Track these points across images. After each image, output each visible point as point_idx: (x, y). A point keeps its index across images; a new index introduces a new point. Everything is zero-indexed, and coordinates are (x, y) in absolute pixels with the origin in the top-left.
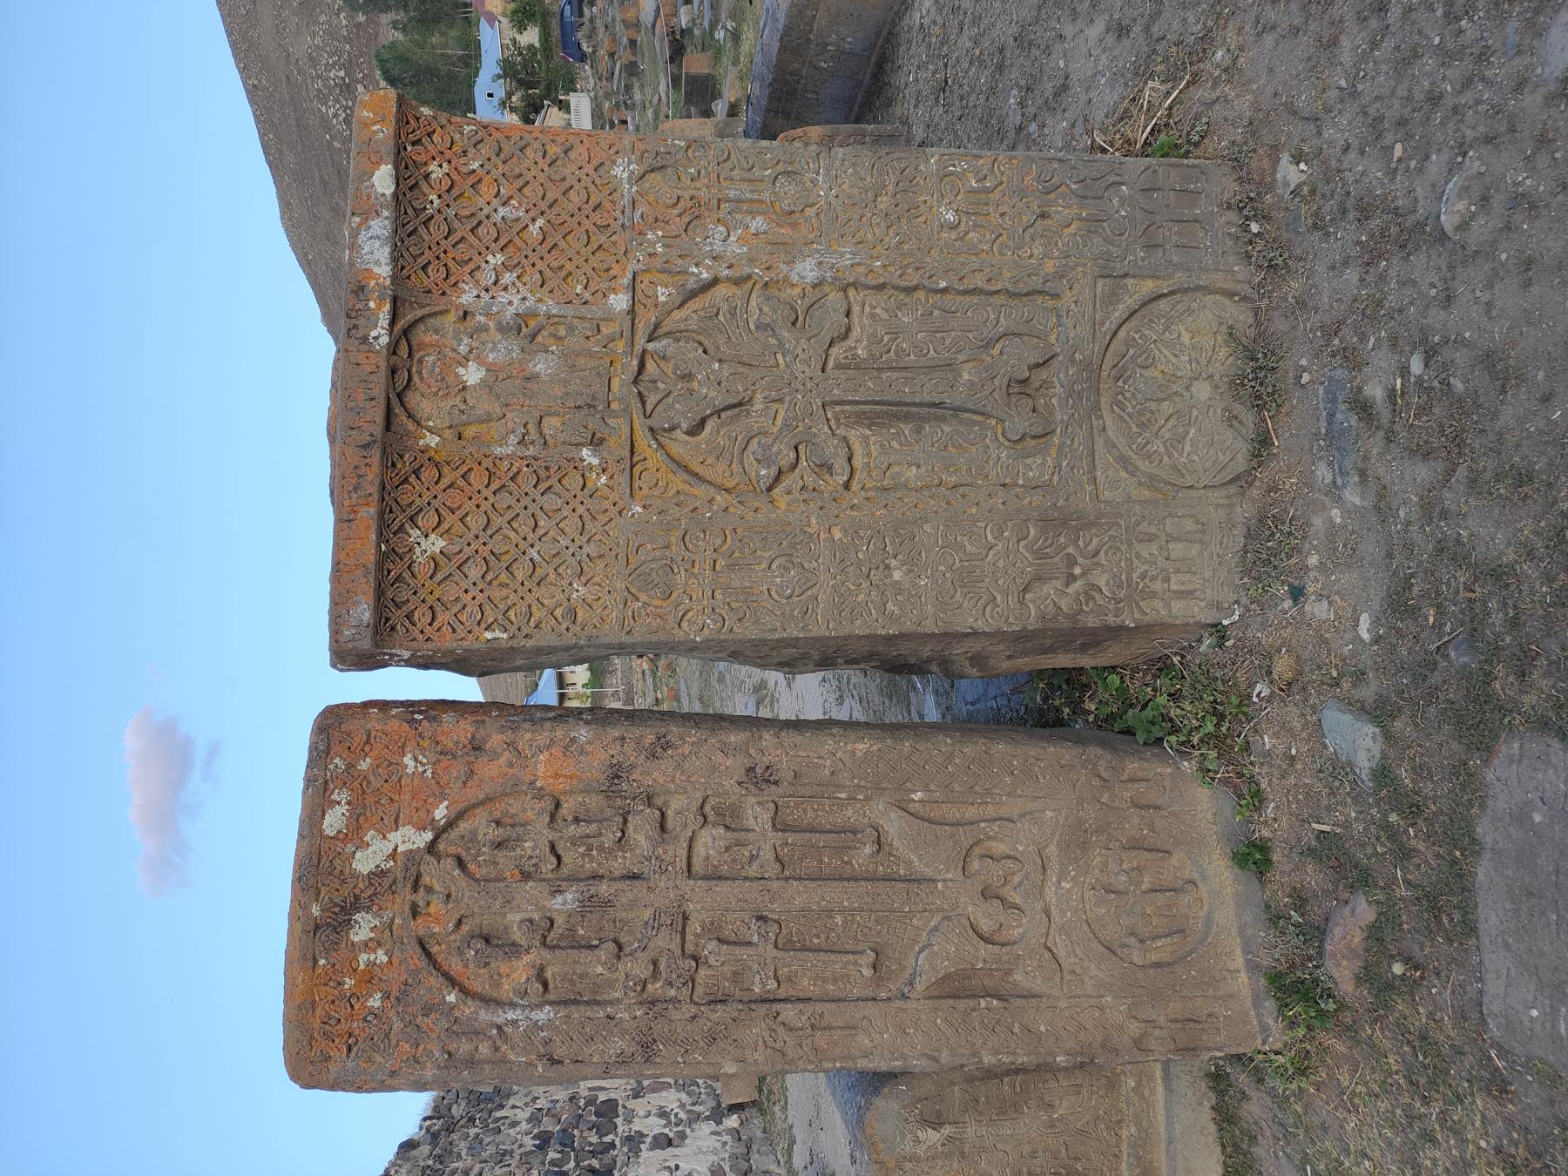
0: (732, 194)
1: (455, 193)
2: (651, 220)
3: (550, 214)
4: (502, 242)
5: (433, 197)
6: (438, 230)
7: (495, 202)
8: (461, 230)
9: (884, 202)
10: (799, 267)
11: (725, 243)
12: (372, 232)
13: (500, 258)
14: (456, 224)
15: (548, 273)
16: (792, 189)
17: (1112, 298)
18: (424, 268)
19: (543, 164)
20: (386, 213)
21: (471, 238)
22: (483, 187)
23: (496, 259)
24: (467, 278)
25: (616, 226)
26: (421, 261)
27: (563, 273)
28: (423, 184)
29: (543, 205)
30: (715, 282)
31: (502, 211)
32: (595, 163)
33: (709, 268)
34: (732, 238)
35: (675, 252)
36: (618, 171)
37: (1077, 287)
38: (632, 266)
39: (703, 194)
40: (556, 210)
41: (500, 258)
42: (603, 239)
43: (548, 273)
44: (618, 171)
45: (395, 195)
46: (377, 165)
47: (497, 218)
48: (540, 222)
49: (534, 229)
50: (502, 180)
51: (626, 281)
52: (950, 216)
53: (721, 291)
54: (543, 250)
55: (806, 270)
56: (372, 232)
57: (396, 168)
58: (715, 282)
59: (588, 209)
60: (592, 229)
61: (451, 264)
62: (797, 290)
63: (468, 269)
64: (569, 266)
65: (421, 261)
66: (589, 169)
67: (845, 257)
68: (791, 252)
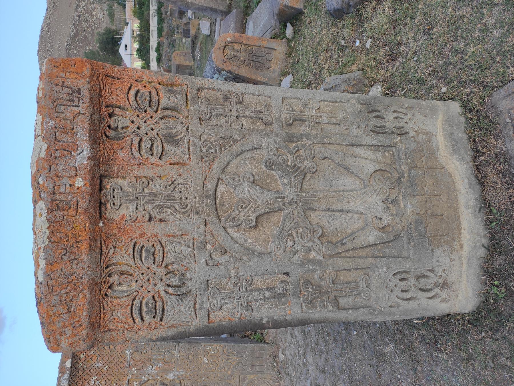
0: (154, 356)
1: (86, 361)
2: (134, 365)
3: (109, 365)
4: (97, 373)
5: (81, 363)
6: (81, 372)
7: (96, 362)
8: (87, 371)
9: (191, 357)
10: (169, 375)
11: (151, 370)
12: (64, 378)
13: (96, 377)
14: (86, 369)
15: (107, 381)
16: (169, 355)
17: (244, 379)
18: (76, 384)
19: (109, 351)
20: (68, 372)
21: (89, 373)
22: (93, 359)
23: (95, 378)
24: (87, 384)
25: (125, 367)
26: (76, 382)
27: (111, 381)
28: (79, 361)
29: (108, 362)
30: (149, 380)
31: (97, 365)
32: (121, 350)
33: (147, 377)
34: (154, 369)
35: (139, 373)
36: (127, 352)
37: (235, 378)
38: (128, 378)
39: (147, 358)
40: (111, 364)
41: (96, 377)
42: (122, 371)
43: (107, 381)
44: (127, 352)
45: (71, 367)
46: (67, 359)
47: (96, 367)
48: (107, 367)
49: (105, 369)
50: (98, 356)
51: (126, 382)
52: (206, 361)
53: (150, 382)
54: (106, 375)
55: (171, 376)
56: (64, 378)
57: (72, 360)
58: (149, 380)
59: (119, 362)
60: (119, 368)
61: (83, 380)
62: (169, 381)
63: (87, 381)
64: (113, 379)
65: (76, 382)
66: (120, 352)
67: (181, 372)
68: (167, 371)
